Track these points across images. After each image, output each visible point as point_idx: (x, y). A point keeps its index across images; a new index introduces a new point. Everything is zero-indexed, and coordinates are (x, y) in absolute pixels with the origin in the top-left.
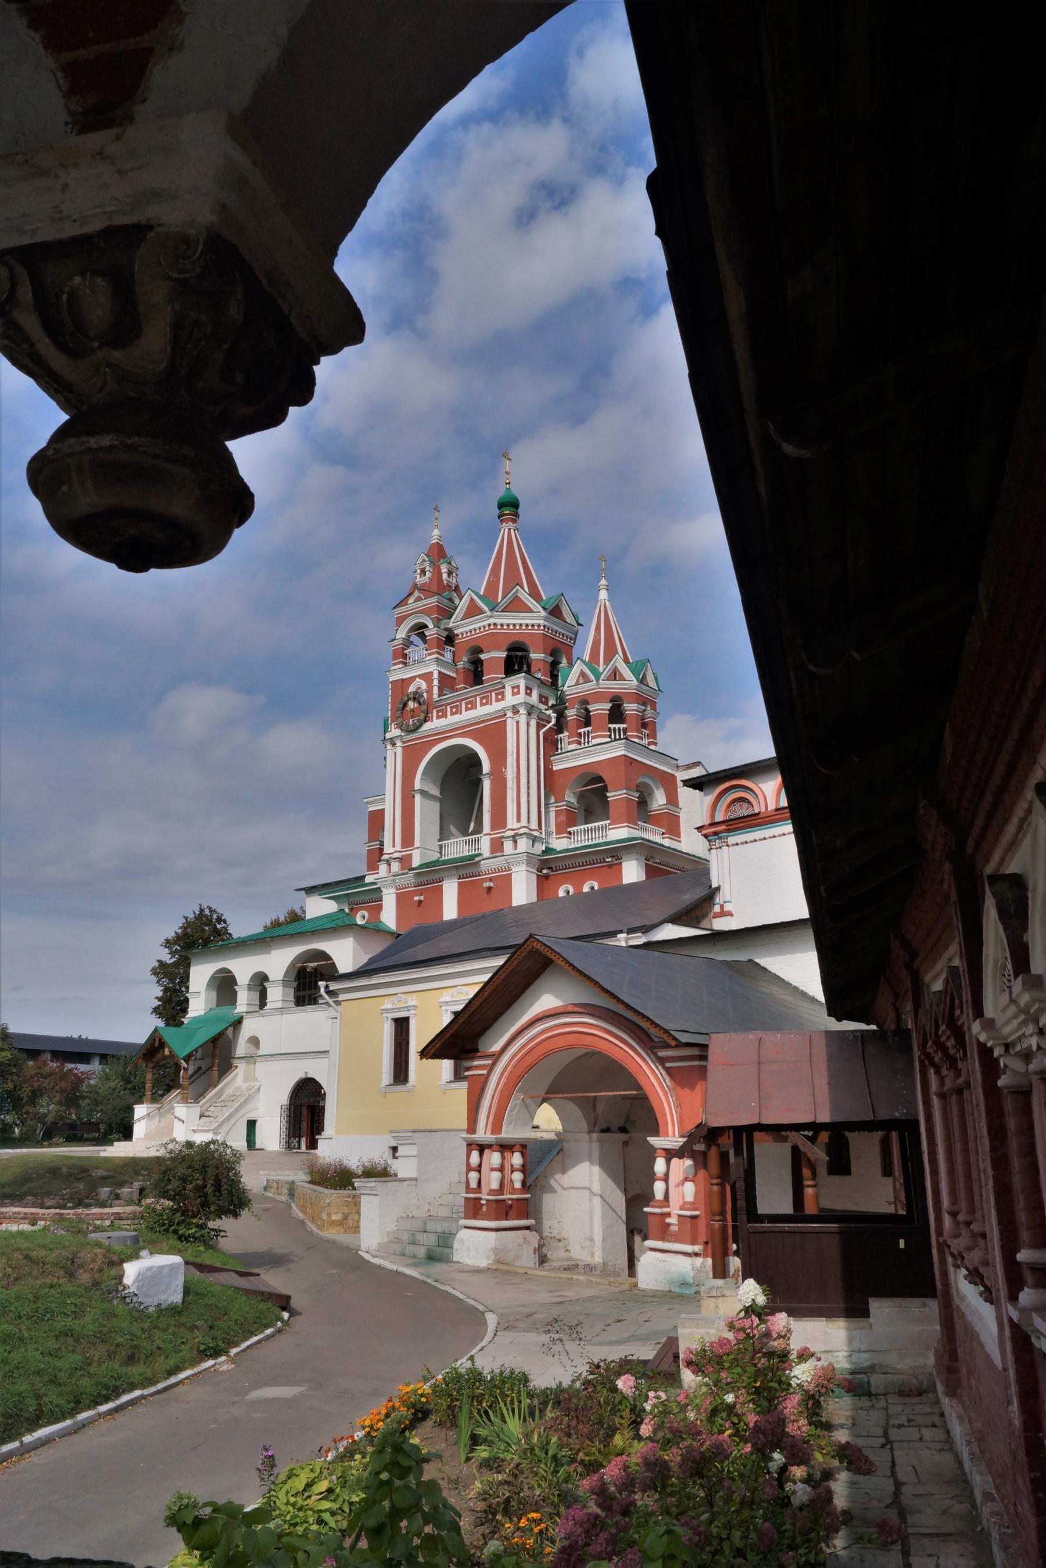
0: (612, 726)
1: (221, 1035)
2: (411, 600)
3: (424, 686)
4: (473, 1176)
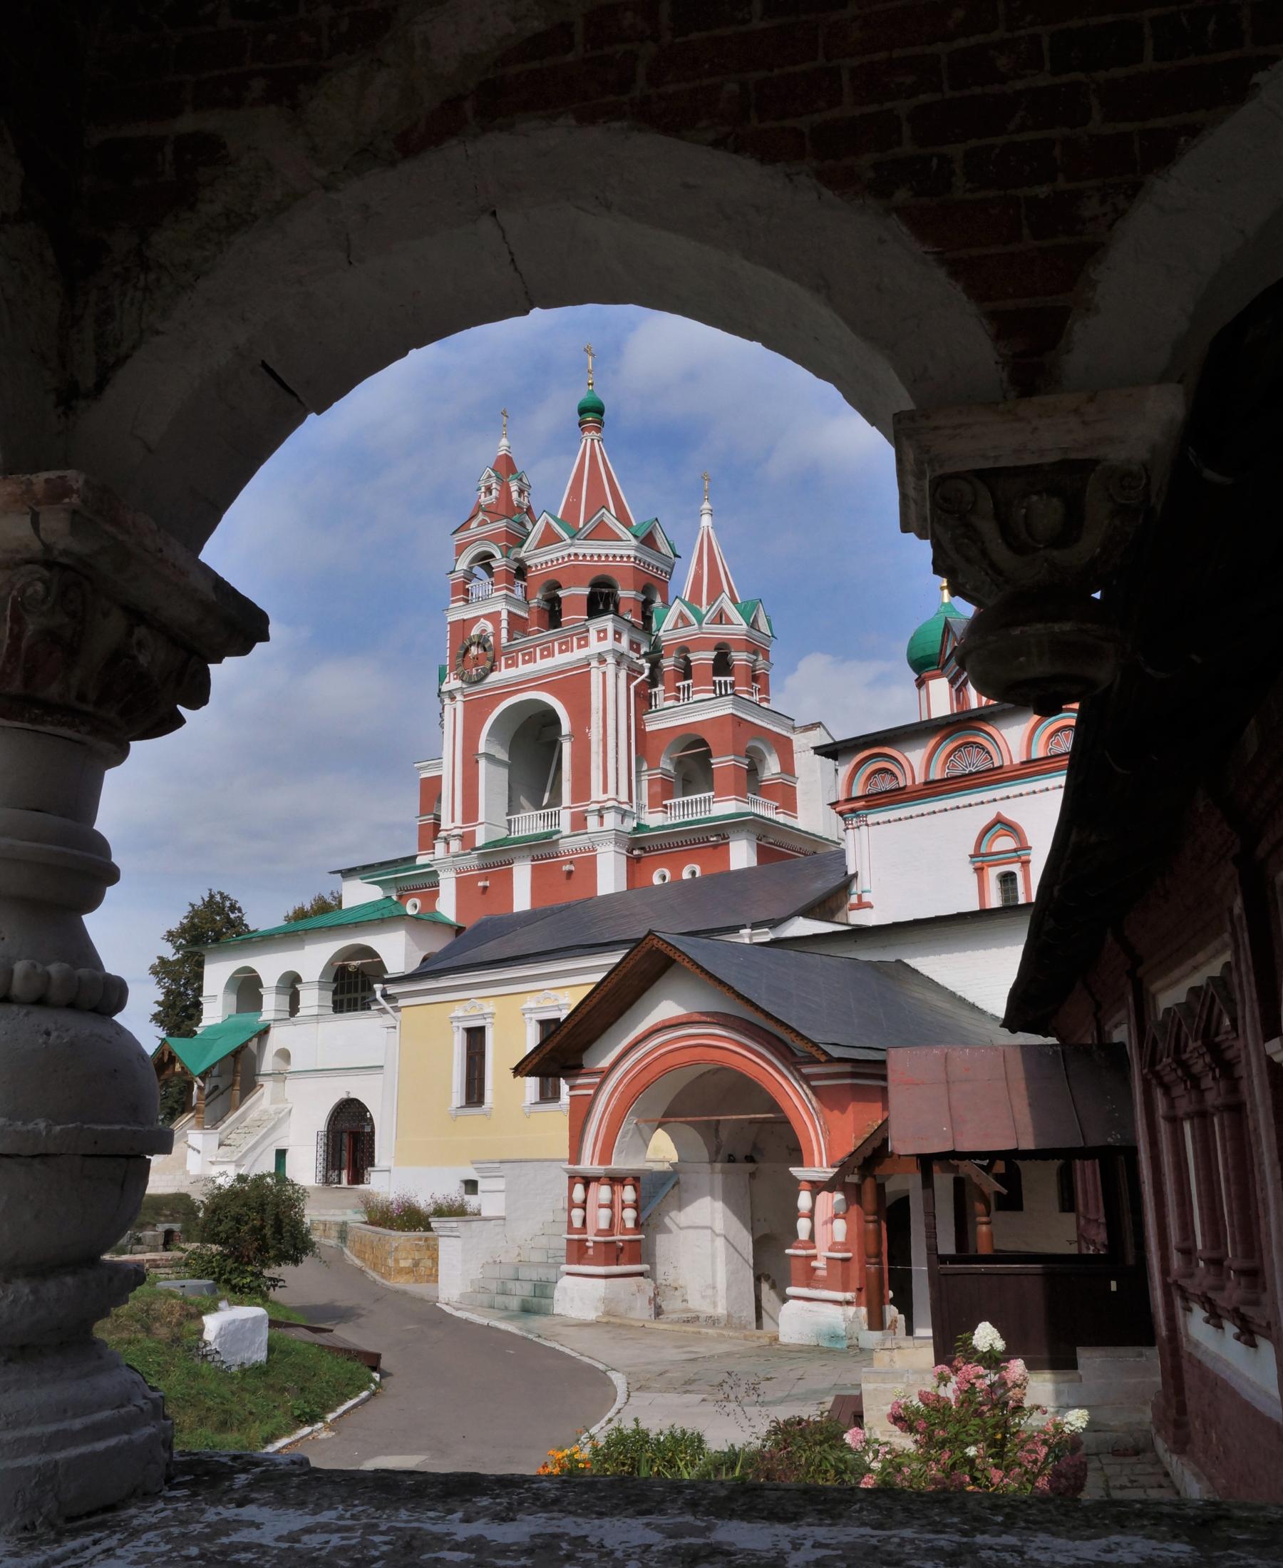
0: (717, 679)
1: (244, 1046)
2: (474, 524)
3: (490, 628)
4: (577, 1213)
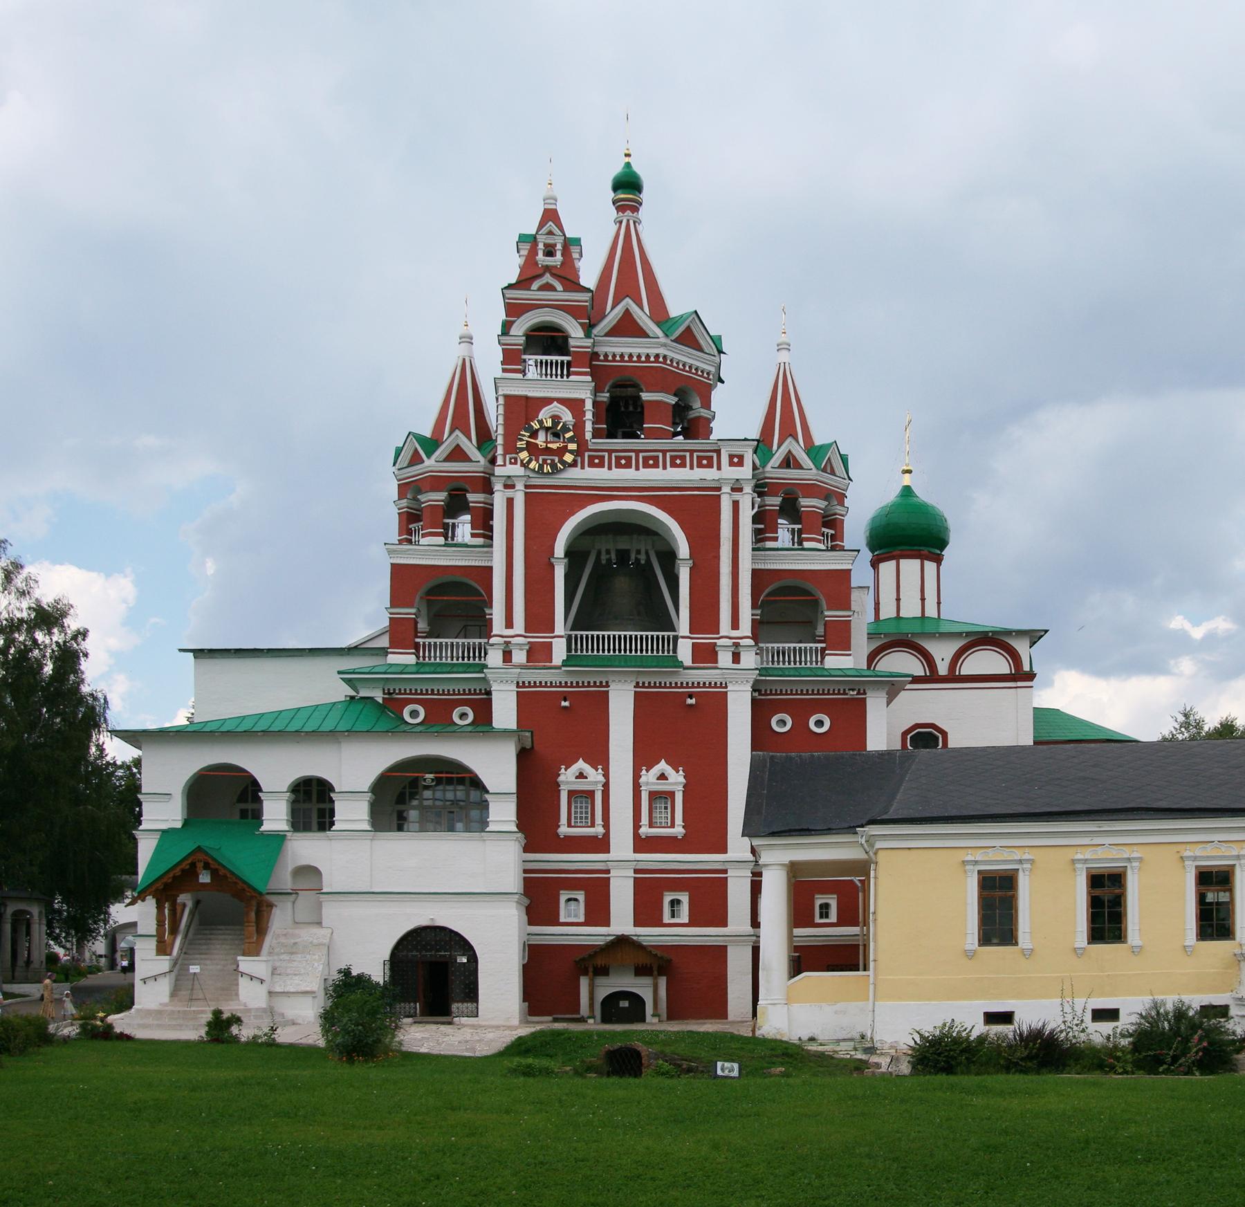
2: (535, 286)
3: (567, 417)
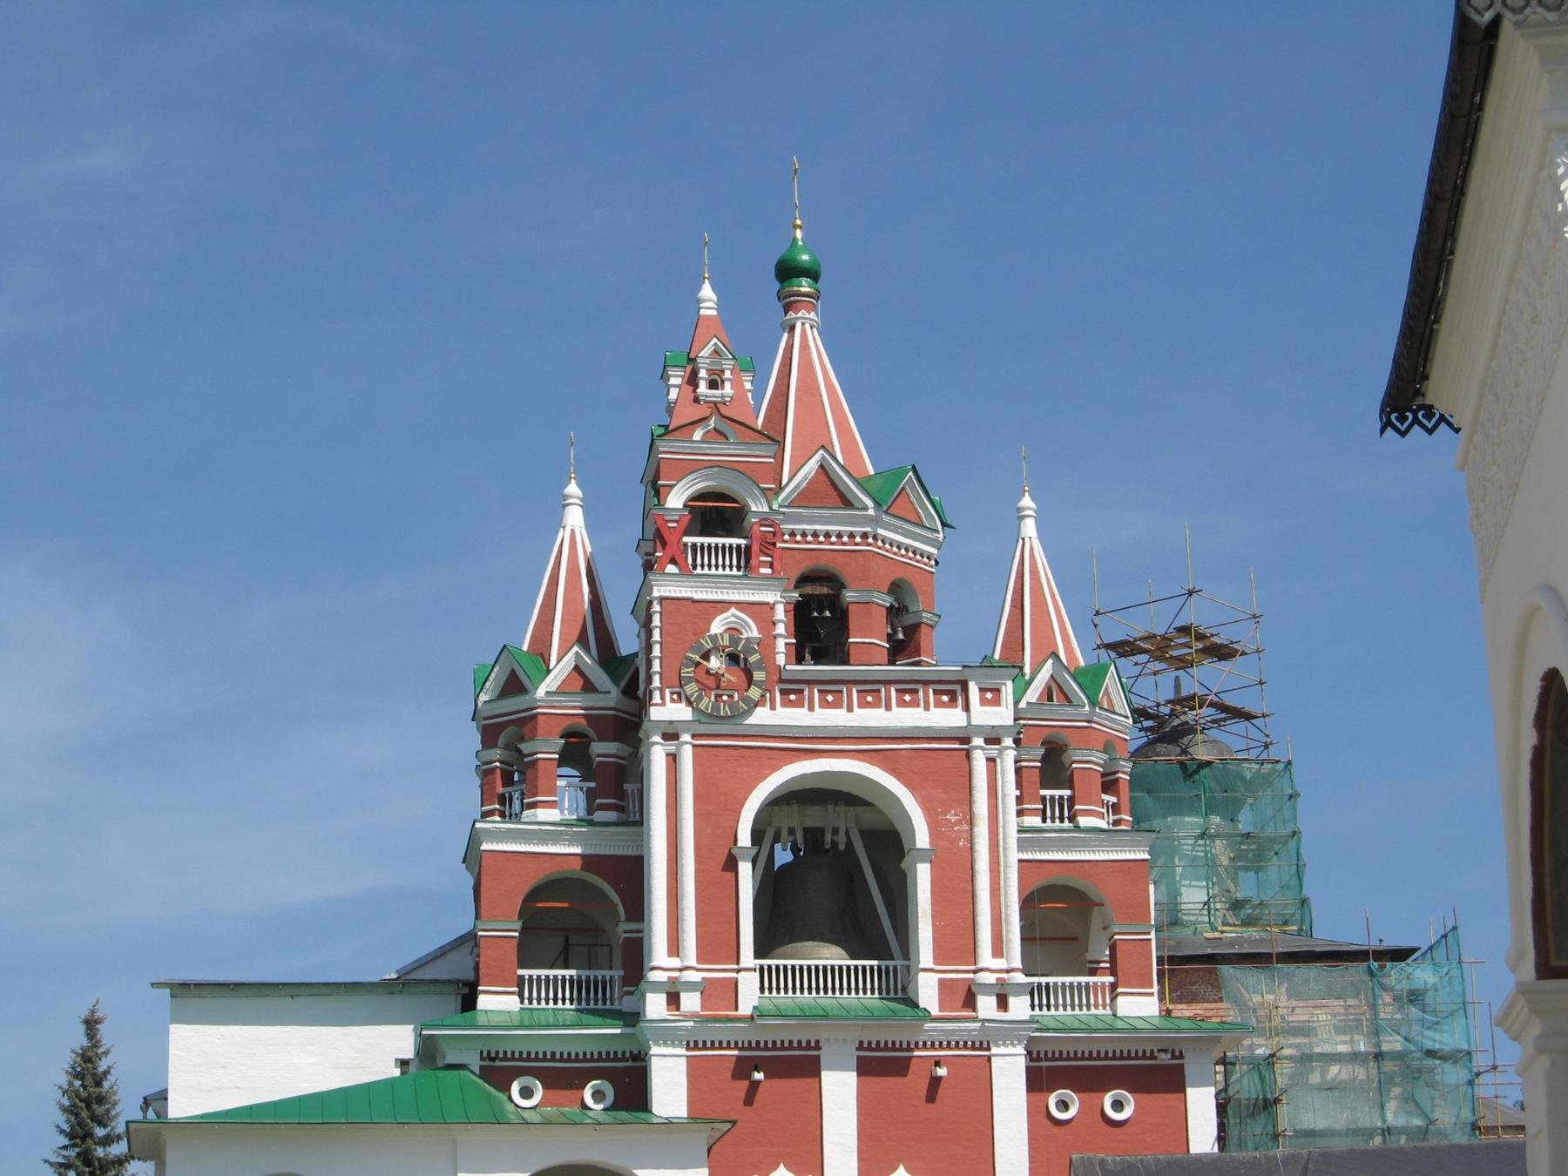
2: (697, 435)
